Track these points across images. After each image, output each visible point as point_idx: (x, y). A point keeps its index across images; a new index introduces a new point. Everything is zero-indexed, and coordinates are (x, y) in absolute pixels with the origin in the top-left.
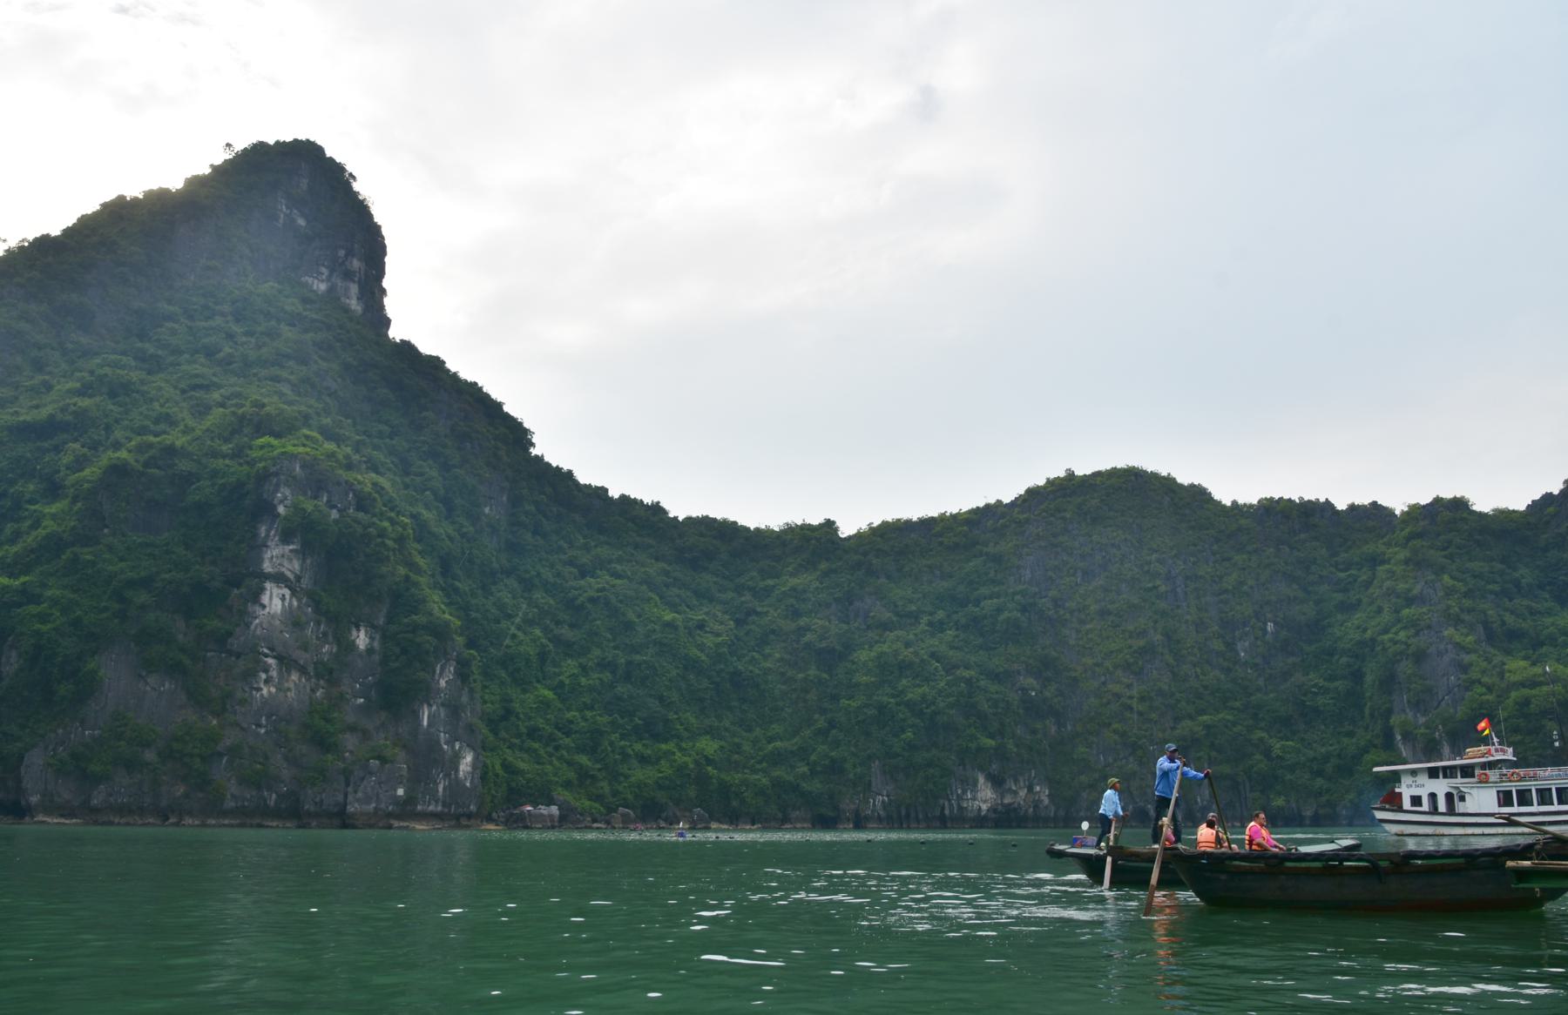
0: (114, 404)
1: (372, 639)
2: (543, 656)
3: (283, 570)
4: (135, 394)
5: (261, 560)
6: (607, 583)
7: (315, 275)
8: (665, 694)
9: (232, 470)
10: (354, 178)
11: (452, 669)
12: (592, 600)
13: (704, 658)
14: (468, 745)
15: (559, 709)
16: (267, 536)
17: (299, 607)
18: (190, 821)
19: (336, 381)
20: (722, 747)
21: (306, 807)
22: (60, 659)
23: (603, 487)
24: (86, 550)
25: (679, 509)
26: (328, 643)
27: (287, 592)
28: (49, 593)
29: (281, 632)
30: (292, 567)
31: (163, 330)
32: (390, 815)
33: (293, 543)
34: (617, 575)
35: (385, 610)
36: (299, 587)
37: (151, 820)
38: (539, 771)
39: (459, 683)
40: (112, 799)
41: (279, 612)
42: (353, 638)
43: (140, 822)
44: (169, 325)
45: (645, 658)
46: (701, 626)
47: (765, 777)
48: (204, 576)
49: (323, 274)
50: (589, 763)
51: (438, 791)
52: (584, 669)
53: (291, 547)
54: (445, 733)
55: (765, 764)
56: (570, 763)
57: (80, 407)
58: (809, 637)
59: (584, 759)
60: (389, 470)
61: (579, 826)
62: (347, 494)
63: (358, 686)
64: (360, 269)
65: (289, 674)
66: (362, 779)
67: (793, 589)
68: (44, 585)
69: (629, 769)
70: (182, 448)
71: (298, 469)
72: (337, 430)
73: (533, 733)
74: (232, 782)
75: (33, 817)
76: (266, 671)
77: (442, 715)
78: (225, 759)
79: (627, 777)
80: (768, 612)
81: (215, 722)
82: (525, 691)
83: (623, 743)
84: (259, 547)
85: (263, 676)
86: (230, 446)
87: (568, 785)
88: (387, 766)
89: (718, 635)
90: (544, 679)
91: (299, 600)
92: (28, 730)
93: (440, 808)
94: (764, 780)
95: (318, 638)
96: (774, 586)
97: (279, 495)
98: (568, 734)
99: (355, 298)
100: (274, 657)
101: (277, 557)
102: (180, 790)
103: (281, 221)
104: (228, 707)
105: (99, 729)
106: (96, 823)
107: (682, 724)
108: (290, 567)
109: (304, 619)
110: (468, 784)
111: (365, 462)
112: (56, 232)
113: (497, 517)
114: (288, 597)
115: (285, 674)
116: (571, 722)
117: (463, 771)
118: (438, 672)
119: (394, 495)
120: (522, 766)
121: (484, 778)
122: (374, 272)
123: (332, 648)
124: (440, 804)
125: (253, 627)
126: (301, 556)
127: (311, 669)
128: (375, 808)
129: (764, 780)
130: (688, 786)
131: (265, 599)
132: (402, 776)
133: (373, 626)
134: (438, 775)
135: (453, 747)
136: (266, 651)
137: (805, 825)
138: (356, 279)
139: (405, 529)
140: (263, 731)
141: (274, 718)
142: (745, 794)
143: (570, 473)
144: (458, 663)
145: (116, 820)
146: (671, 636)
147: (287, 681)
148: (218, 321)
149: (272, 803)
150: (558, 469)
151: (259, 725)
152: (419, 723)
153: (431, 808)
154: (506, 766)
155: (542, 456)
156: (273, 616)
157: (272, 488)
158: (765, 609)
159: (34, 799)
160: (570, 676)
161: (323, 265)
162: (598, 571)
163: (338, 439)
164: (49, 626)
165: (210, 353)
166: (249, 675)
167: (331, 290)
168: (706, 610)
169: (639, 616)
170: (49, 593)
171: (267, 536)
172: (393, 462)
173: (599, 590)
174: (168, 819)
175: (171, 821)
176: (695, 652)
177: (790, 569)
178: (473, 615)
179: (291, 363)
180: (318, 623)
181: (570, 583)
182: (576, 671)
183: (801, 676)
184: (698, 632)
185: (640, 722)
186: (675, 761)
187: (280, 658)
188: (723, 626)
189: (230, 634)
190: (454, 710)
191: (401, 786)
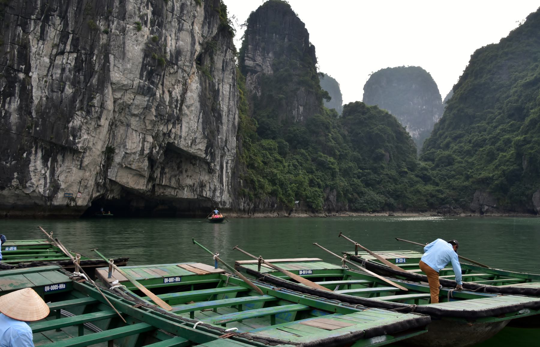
28: (534, 139)
68: (532, 137)
170: (534, 139)
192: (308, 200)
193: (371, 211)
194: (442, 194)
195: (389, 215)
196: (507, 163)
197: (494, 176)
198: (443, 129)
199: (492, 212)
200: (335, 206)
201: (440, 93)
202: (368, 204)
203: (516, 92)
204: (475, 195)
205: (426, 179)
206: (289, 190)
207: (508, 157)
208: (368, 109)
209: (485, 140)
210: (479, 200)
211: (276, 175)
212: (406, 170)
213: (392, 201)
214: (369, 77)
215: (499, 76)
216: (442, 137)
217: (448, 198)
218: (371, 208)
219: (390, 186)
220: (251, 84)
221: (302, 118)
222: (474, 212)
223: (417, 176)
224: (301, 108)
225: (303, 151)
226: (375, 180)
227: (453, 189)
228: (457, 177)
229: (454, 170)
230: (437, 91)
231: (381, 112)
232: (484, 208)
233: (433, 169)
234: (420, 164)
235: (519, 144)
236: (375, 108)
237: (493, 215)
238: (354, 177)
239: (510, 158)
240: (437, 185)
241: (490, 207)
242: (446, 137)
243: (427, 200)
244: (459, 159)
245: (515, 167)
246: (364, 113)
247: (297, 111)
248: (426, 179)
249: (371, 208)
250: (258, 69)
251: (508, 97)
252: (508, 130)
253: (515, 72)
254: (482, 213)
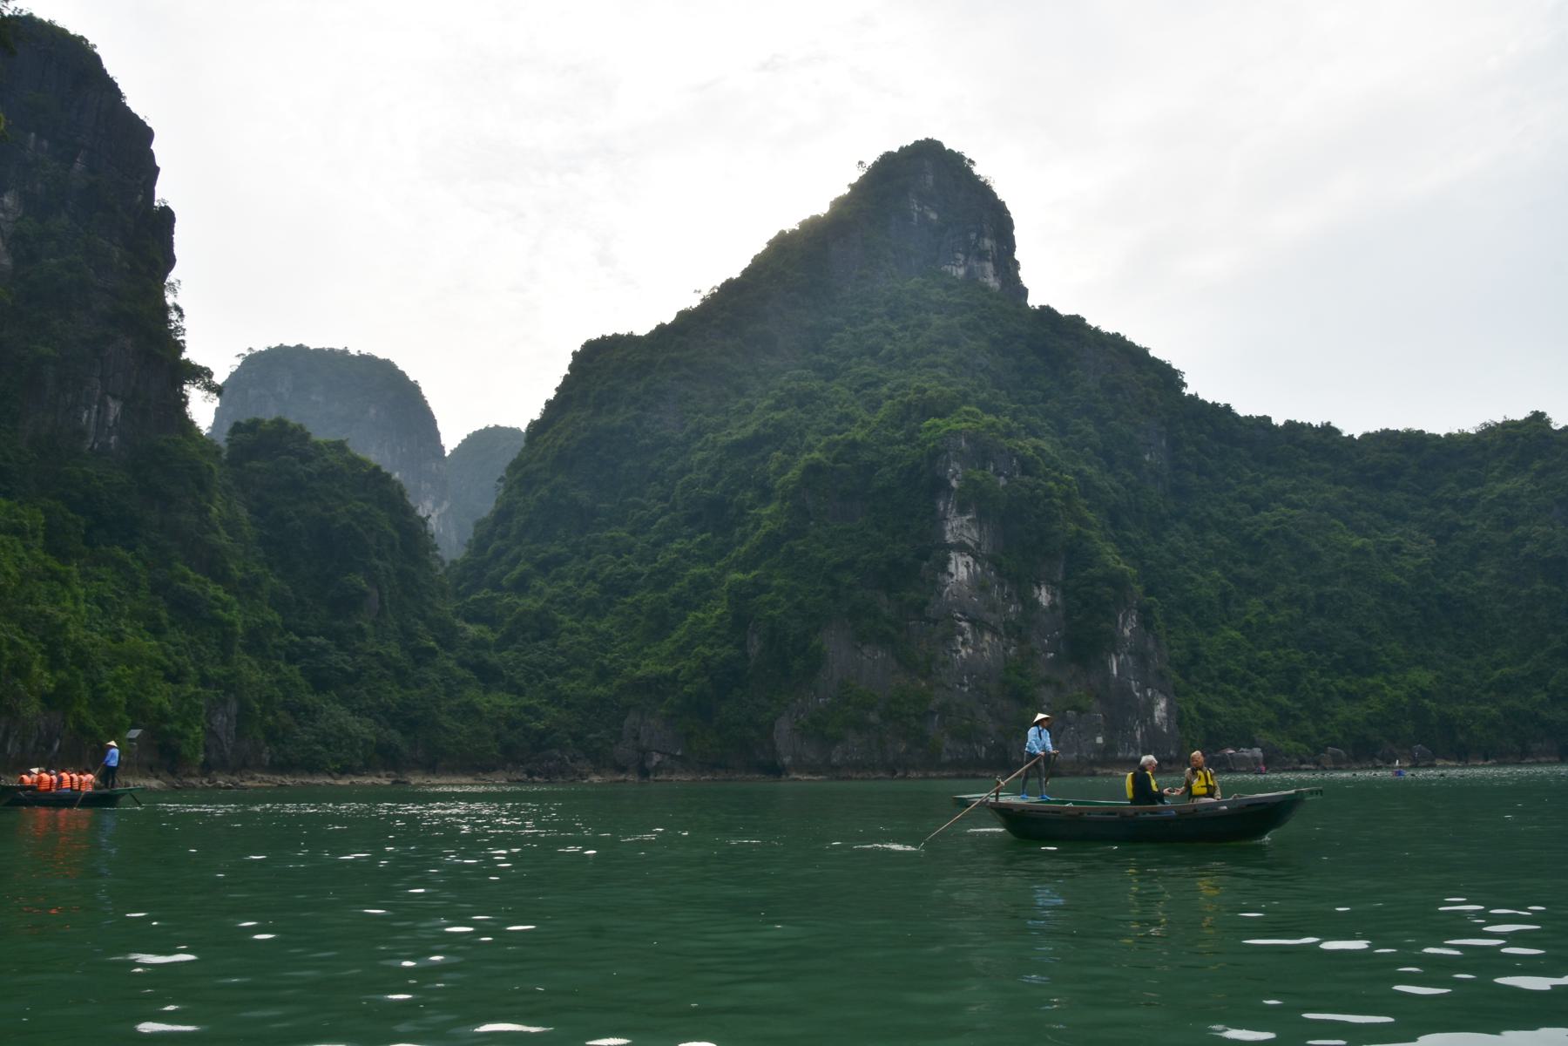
0: (803, 413)
1: (1053, 595)
2: (1225, 597)
3: (964, 539)
4: (818, 401)
5: (944, 533)
6: (1284, 515)
7: (953, 262)
8: (1364, 625)
9: (907, 454)
10: (973, 162)
11: (1134, 617)
12: (1270, 534)
13: (1404, 582)
14: (1160, 691)
15: (1250, 650)
16: (946, 509)
17: (983, 571)
18: (915, 774)
19: (986, 357)
20: (1438, 677)
21: (1014, 758)
22: (791, 639)
23: (1265, 416)
24: (799, 542)
25: (1353, 426)
26: (1013, 603)
27: (970, 559)
28: (775, 583)
29: (970, 597)
30: (971, 536)
31: (833, 340)
32: (1092, 763)
33: (969, 513)
34: (1295, 506)
35: (1062, 566)
36: (981, 553)
37: (882, 775)
38: (1237, 714)
39: (1143, 630)
40: (848, 757)
41: (966, 578)
42: (1035, 596)
43: (874, 776)
44: (836, 335)
45: (1336, 589)
46: (1397, 548)
47: (1494, 707)
48: (897, 553)
49: (959, 260)
50: (1289, 703)
51: (1136, 738)
52: (1270, 606)
53: (968, 517)
54: (1136, 681)
55: (1492, 694)
56: (1268, 704)
57: (777, 420)
58: (1529, 547)
59: (1283, 699)
60: (1047, 432)
61: (1287, 768)
62: (1011, 460)
63: (1046, 641)
64: (992, 247)
65: (983, 636)
66: (1062, 729)
67: (1503, 496)
69: (1334, 706)
70: (863, 440)
71: (963, 443)
72: (993, 403)
73: (1225, 676)
74: (946, 737)
75: (787, 775)
76: (962, 634)
77: (1131, 663)
78: (937, 718)
79: (1332, 715)
80: (1474, 525)
81: (924, 684)
82: (1211, 634)
83: (1323, 680)
84: (939, 520)
85: (960, 639)
86: (902, 432)
87: (1269, 726)
88: (1084, 716)
89: (1418, 556)
90: (1229, 620)
91: (982, 566)
92: (775, 701)
94: (1494, 711)
95: (1004, 599)
96: (1479, 495)
97: (951, 470)
98: (1261, 674)
99: (992, 276)
100: (967, 621)
101: (957, 528)
102: (903, 747)
103: (916, 219)
104: (934, 669)
105: (830, 696)
106: (838, 778)
107: (1387, 656)
108: (969, 536)
109: (989, 583)
110: (1165, 730)
111: (1024, 428)
112: (736, 274)
113: (1159, 463)
114: (971, 564)
115: (979, 636)
116: (1264, 661)
117: (1158, 717)
118: (1121, 621)
119: (1055, 455)
120: (1218, 709)
121: (1180, 723)
122: (1005, 247)
123: (1018, 608)
124: (1139, 750)
125: (944, 595)
126: (978, 524)
127: (1001, 629)
128: (1078, 757)
129: (1494, 711)
130: (1403, 721)
131: (952, 568)
132: (1099, 724)
133: (1052, 583)
134: (1135, 723)
135: (1146, 695)
136: (959, 615)
137: (1551, 759)
138: (990, 258)
139: (1070, 487)
140: (966, 689)
141: (974, 676)
142: (1473, 727)
143: (1228, 407)
144: (1139, 611)
145: (854, 776)
146: (1363, 563)
147: (981, 642)
148: (876, 322)
149: (983, 755)
150: (1215, 405)
151: (962, 684)
152: (1109, 671)
154: (1199, 709)
155: (1196, 394)
156: (960, 583)
157: (943, 465)
158: (1471, 522)
159: (787, 760)
160: (1257, 615)
161: (959, 251)
162: (1273, 504)
163: (996, 411)
164: (779, 611)
165: (873, 352)
166: (948, 639)
167: (969, 273)
168: (1400, 530)
169: (1324, 545)
170: (775, 583)
171: (946, 509)
172: (1049, 425)
173: (1275, 524)
174: (895, 773)
175: (898, 774)
176: (1393, 577)
177: (1495, 474)
178: (1149, 562)
179: (944, 348)
180: (1002, 585)
181: (1245, 519)
182: (1262, 609)
183: (1524, 592)
184: (1394, 555)
185: (1340, 657)
186: (1386, 695)
187: (972, 621)
188: (1422, 546)
189: (926, 603)
190: (1142, 658)
191: (1100, 734)
192: (167, 727)
193: (336, 770)
194: (538, 718)
195: (394, 783)
196: (711, 640)
197: (678, 671)
198: (503, 536)
199: (673, 772)
200: (228, 751)
201: (442, 443)
202: (327, 745)
203: (704, 462)
204: (627, 722)
205: (488, 676)
206: (106, 689)
207: (711, 623)
208: (316, 445)
209: (635, 576)
210: (637, 738)
211: (63, 626)
212: (432, 644)
213: (395, 736)
214: (239, 362)
215: (657, 416)
216: (504, 558)
217: (555, 731)
218: (337, 760)
219: (390, 692)
221: (113, 439)
222: (622, 769)
223: (462, 664)
224: (115, 408)
225: (120, 552)
226: (342, 670)
227: (568, 706)
228: (571, 671)
229: (562, 653)
230: (436, 435)
231: (356, 462)
232: (651, 759)
233: (500, 646)
234: (464, 629)
235: (742, 592)
236: (340, 446)
237: (674, 778)
238: (278, 658)
239: (717, 628)
240: (520, 692)
241: (666, 757)
242: (515, 561)
243: (497, 737)
244: (567, 621)
245: (728, 651)
246: (306, 458)
247: (99, 412)
248: (488, 676)
249: (337, 760)
251: (682, 472)
252: (694, 555)
253: (696, 413)
254: (644, 772)
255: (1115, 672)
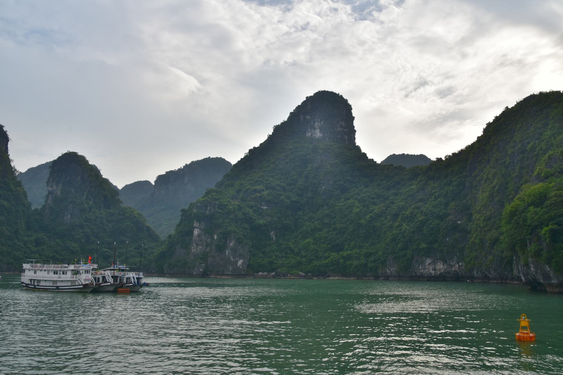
27: (198, 230)
51: (230, 269)
64: (318, 125)
85: (193, 247)
91: (201, 231)
93: (231, 273)
95: (206, 238)
100: (195, 243)
114: (199, 231)
131: (194, 232)
134: (229, 266)
152: (226, 255)
153: (228, 273)
220: (51, 200)
224: (69, 216)
250: (55, 192)
255: (227, 254)
